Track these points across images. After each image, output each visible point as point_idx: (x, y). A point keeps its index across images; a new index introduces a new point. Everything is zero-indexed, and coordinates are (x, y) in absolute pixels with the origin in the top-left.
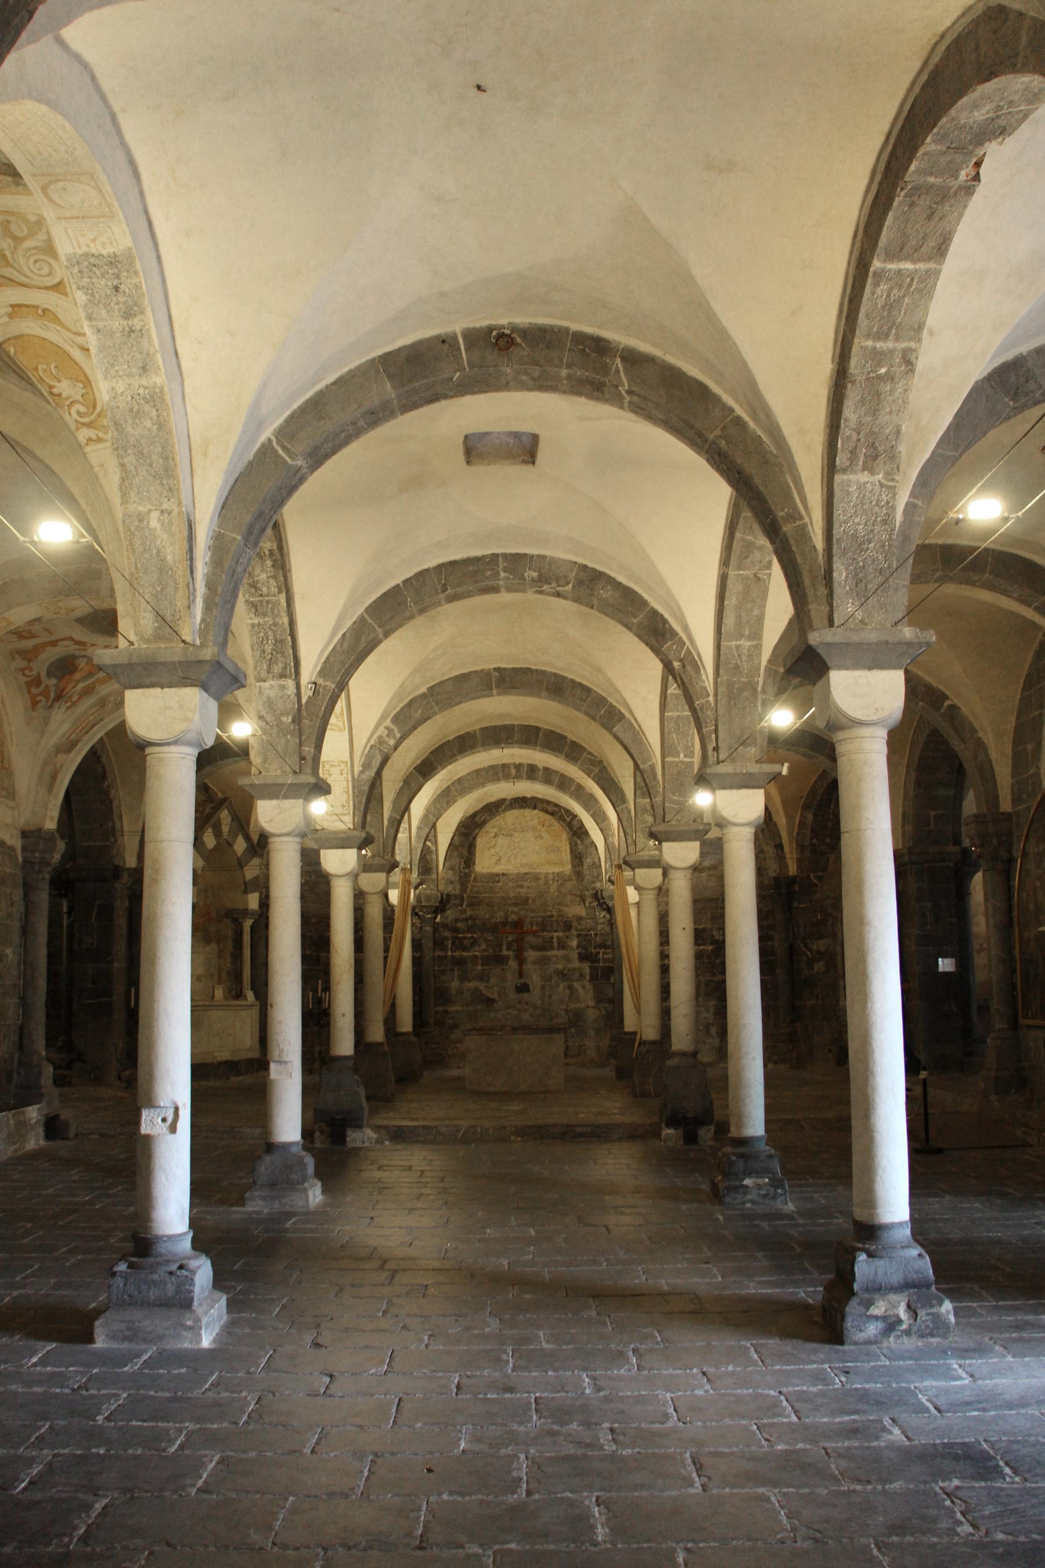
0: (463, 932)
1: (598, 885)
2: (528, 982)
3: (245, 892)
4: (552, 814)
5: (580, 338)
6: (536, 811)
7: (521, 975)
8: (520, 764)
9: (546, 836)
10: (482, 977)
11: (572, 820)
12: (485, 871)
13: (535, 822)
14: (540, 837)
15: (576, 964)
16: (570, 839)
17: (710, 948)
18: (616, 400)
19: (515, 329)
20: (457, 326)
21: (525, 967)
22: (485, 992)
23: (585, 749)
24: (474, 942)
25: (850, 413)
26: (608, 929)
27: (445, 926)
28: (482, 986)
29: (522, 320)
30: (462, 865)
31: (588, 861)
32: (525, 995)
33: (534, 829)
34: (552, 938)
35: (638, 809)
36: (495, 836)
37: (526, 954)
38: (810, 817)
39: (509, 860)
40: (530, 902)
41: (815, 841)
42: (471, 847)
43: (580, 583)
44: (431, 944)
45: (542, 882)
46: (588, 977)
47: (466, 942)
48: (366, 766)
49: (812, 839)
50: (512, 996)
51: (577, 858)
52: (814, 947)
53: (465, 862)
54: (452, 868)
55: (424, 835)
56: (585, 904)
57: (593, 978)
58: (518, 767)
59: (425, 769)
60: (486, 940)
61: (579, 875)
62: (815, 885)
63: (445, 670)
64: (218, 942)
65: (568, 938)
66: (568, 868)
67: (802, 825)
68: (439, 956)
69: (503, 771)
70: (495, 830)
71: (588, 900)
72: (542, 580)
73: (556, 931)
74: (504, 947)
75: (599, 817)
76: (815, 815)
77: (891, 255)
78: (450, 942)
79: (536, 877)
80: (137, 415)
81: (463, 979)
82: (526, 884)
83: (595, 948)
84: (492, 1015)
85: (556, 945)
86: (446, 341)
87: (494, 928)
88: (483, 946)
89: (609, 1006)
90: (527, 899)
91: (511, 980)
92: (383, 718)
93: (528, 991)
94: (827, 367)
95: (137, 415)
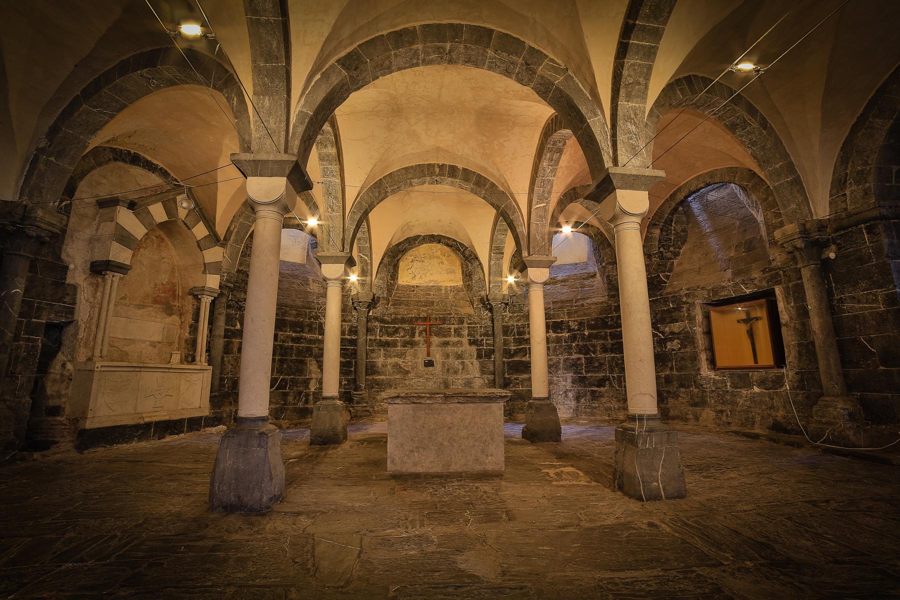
0: (389, 323)
1: (483, 293)
2: (433, 360)
3: (204, 272)
4: (451, 246)
6: (439, 246)
7: (428, 355)
8: (443, 165)
9: (446, 262)
10: (401, 355)
11: (464, 250)
12: (403, 284)
13: (439, 253)
14: (442, 263)
15: (468, 347)
16: (462, 264)
17: (567, 335)
21: (431, 348)
22: (402, 366)
23: (547, 56)
24: (396, 331)
26: (490, 323)
27: (376, 319)
28: (400, 361)
30: (389, 277)
31: (475, 277)
32: (431, 368)
33: (438, 257)
34: (450, 329)
35: (620, 113)
36: (411, 262)
37: (432, 340)
38: (657, 232)
39: (421, 278)
40: (435, 304)
41: (662, 249)
42: (396, 267)
44: (365, 330)
45: (443, 292)
46: (475, 356)
47: (390, 330)
49: (659, 248)
50: (421, 367)
51: (467, 275)
52: (667, 329)
53: (391, 276)
54: (382, 279)
55: (357, 217)
56: (473, 305)
57: (479, 356)
58: (442, 167)
60: (404, 329)
61: (469, 287)
62: (665, 283)
64: (181, 315)
65: (461, 329)
66: (460, 283)
68: (370, 340)
69: (428, 169)
70: (412, 258)
71: (476, 303)
73: (453, 324)
74: (417, 334)
76: (662, 230)
78: (378, 330)
79: (439, 289)
81: (386, 356)
82: (431, 293)
83: (481, 336)
84: (407, 382)
85: (453, 333)
87: (411, 321)
88: (402, 334)
89: (491, 377)
90: (433, 303)
91: (422, 356)
93: (433, 366)
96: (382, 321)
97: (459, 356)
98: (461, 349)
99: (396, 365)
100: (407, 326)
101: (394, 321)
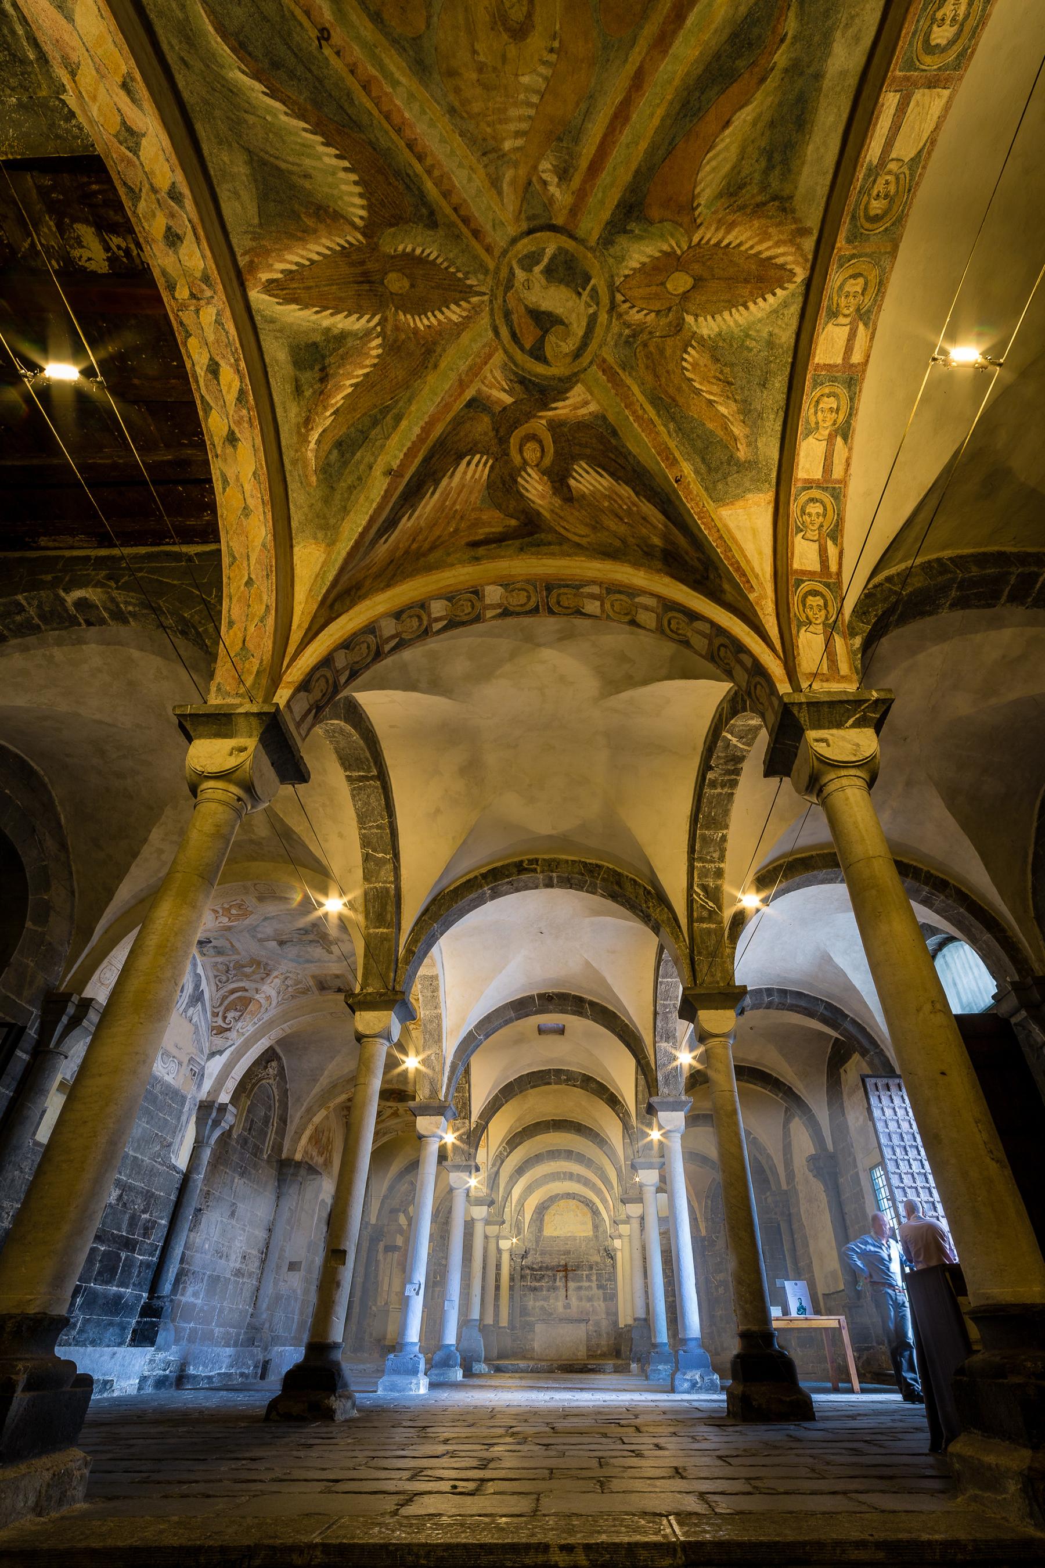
5: (575, 997)
10: (546, 1299)
18: (587, 1017)
19: (553, 993)
20: (535, 993)
25: (659, 1024)
28: (545, 1304)
29: (556, 991)
31: (601, 1229)
43: (583, 1081)
48: (493, 1165)
51: (596, 1227)
57: (605, 1300)
59: (520, 1171)
61: (596, 1237)
63: (530, 1120)
66: (591, 1233)
67: (706, 1206)
72: (568, 1080)
75: (604, 1201)
77: (663, 977)
79: (574, 1239)
80: (431, 1022)
81: (535, 1300)
86: (532, 997)
87: (552, 1269)
92: (502, 1142)
94: (652, 1008)
95: (431, 1022)
96: (532, 1269)
97: (590, 1299)
98: (591, 1293)
99: (542, 1308)
100: (550, 1273)
101: (541, 1269)
